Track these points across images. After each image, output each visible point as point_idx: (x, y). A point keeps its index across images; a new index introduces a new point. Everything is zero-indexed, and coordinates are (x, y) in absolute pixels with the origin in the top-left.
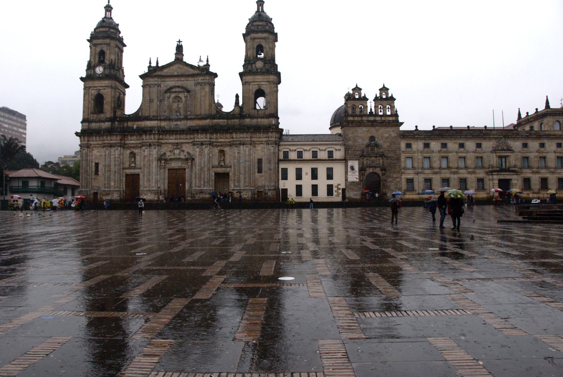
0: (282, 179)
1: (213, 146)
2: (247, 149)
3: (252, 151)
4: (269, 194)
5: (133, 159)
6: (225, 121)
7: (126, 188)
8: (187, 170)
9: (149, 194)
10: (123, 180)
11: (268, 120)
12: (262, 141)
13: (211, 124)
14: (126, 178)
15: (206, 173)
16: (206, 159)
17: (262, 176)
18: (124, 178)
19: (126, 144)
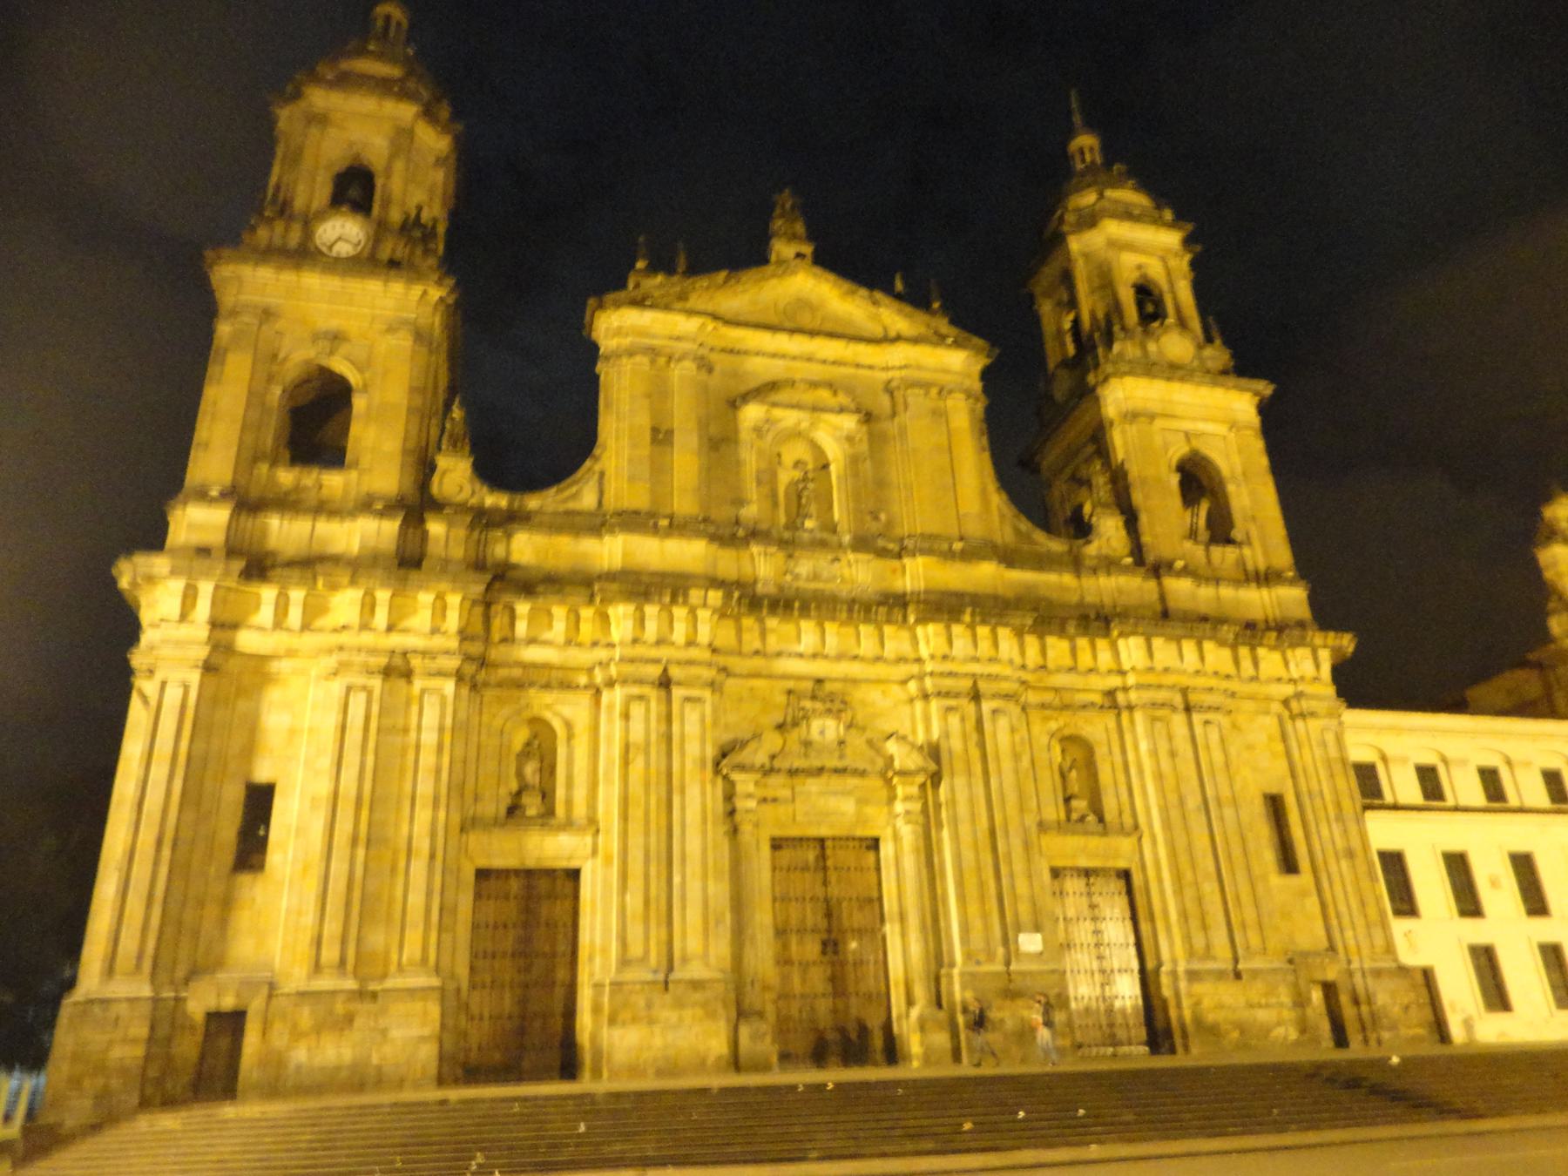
0: (1398, 913)
1: (1024, 709)
2: (1214, 736)
3: (1233, 750)
4: (1382, 999)
5: (530, 769)
6: (1068, 579)
7: (472, 969)
8: (886, 849)
9: (668, 1014)
10: (454, 910)
11: (1265, 592)
12: (1268, 699)
13: (1000, 591)
14: (478, 896)
15: (1019, 866)
16: (1009, 779)
17: (1303, 894)
18: (465, 902)
19: (496, 666)
